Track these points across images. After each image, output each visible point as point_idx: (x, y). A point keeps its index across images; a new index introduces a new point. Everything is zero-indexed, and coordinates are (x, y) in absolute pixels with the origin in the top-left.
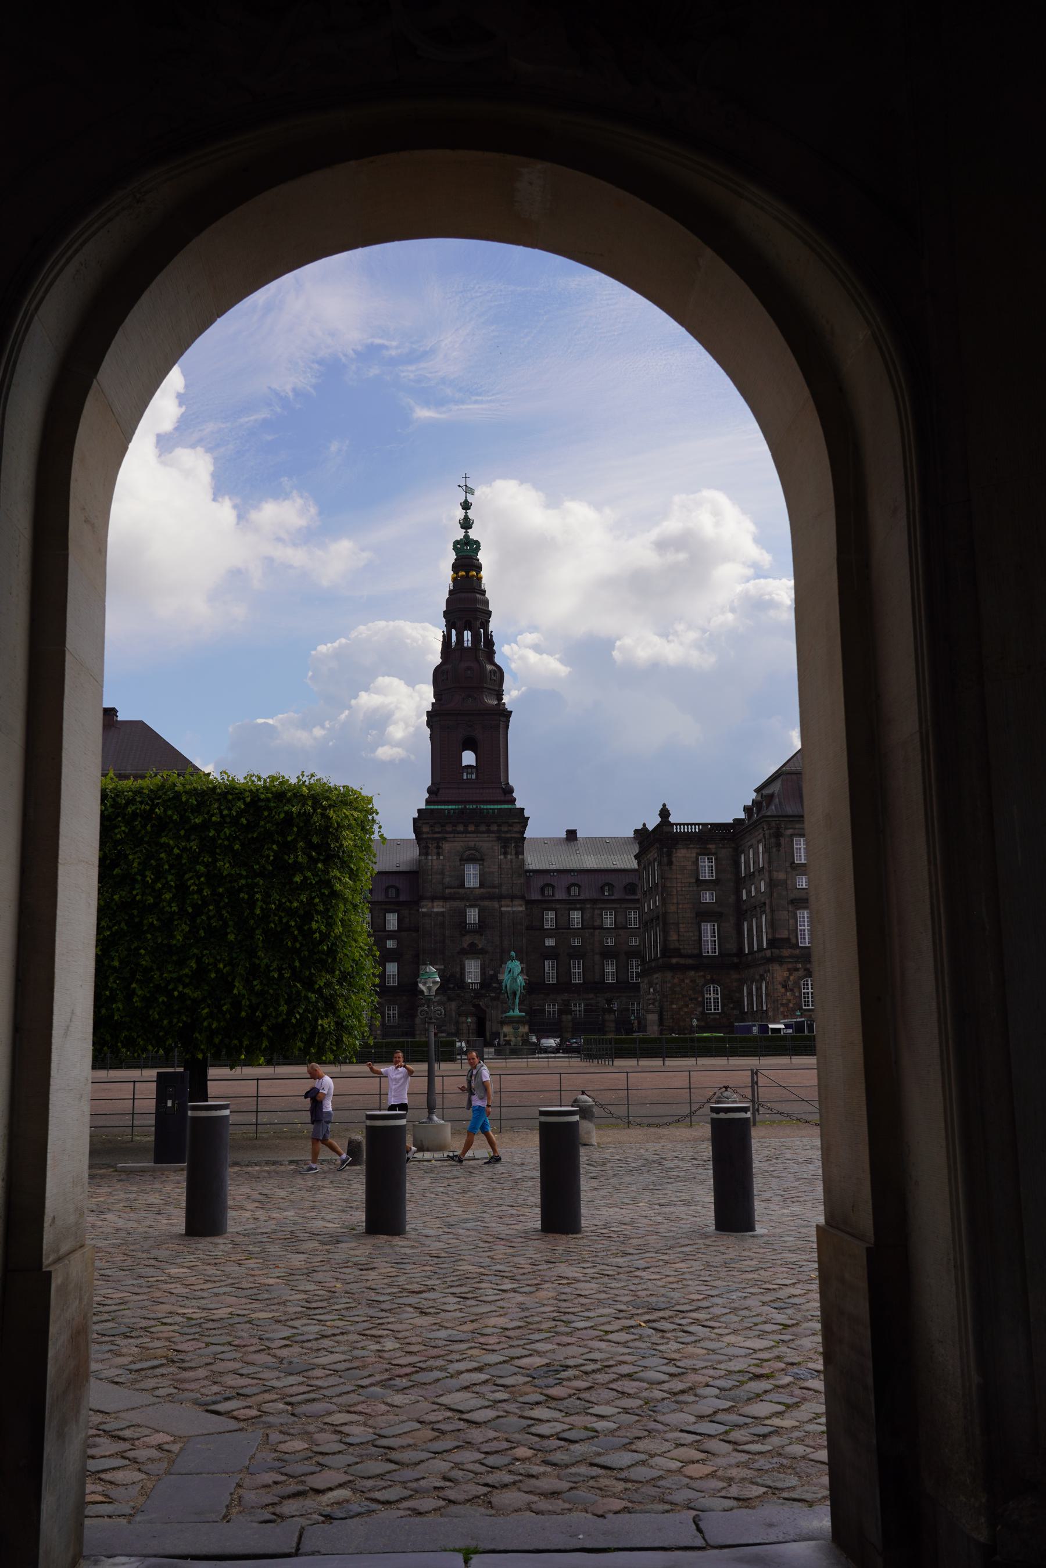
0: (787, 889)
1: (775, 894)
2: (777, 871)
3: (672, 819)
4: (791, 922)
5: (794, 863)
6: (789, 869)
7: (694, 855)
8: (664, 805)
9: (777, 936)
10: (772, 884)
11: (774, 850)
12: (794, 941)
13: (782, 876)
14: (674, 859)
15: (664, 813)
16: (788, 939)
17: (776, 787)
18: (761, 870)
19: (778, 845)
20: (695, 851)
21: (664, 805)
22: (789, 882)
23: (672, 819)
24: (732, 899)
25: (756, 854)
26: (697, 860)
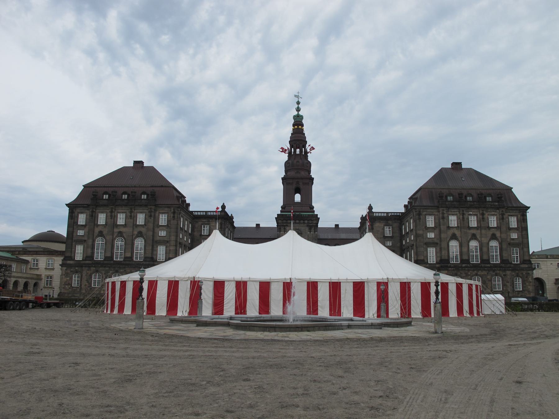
0: (423, 238)
1: (418, 240)
2: (419, 230)
3: (373, 210)
4: (425, 252)
5: (426, 226)
6: (424, 229)
7: (383, 226)
8: (370, 205)
9: (419, 259)
10: (417, 236)
11: (418, 221)
12: (426, 261)
13: (421, 232)
14: (374, 227)
15: (370, 208)
16: (423, 260)
17: (418, 195)
18: (411, 231)
19: (420, 219)
20: (384, 224)
21: (370, 205)
22: (424, 235)
23: (373, 210)
24: (399, 245)
25: (410, 224)
26: (384, 228)
